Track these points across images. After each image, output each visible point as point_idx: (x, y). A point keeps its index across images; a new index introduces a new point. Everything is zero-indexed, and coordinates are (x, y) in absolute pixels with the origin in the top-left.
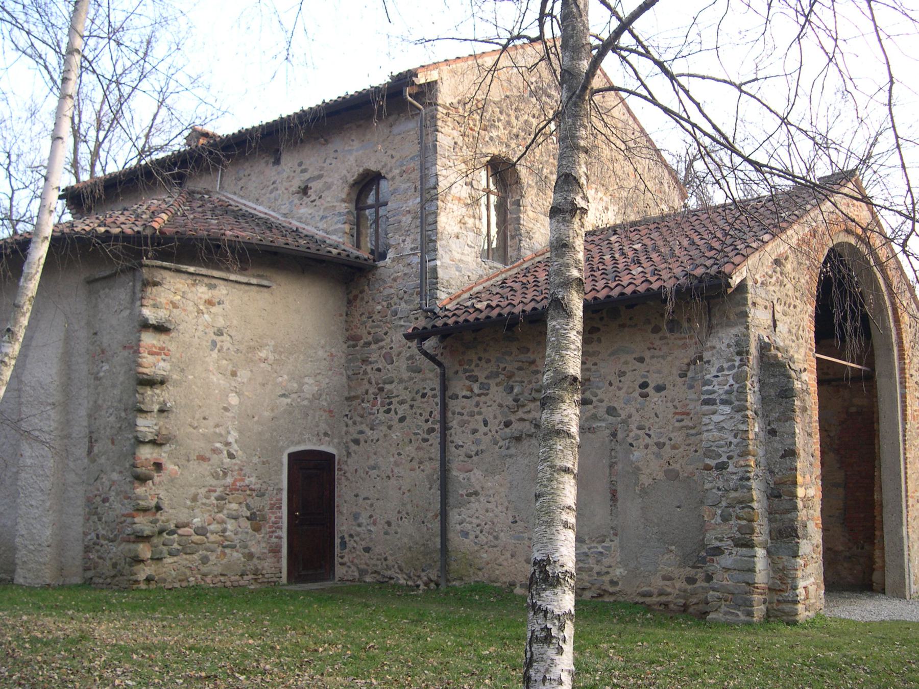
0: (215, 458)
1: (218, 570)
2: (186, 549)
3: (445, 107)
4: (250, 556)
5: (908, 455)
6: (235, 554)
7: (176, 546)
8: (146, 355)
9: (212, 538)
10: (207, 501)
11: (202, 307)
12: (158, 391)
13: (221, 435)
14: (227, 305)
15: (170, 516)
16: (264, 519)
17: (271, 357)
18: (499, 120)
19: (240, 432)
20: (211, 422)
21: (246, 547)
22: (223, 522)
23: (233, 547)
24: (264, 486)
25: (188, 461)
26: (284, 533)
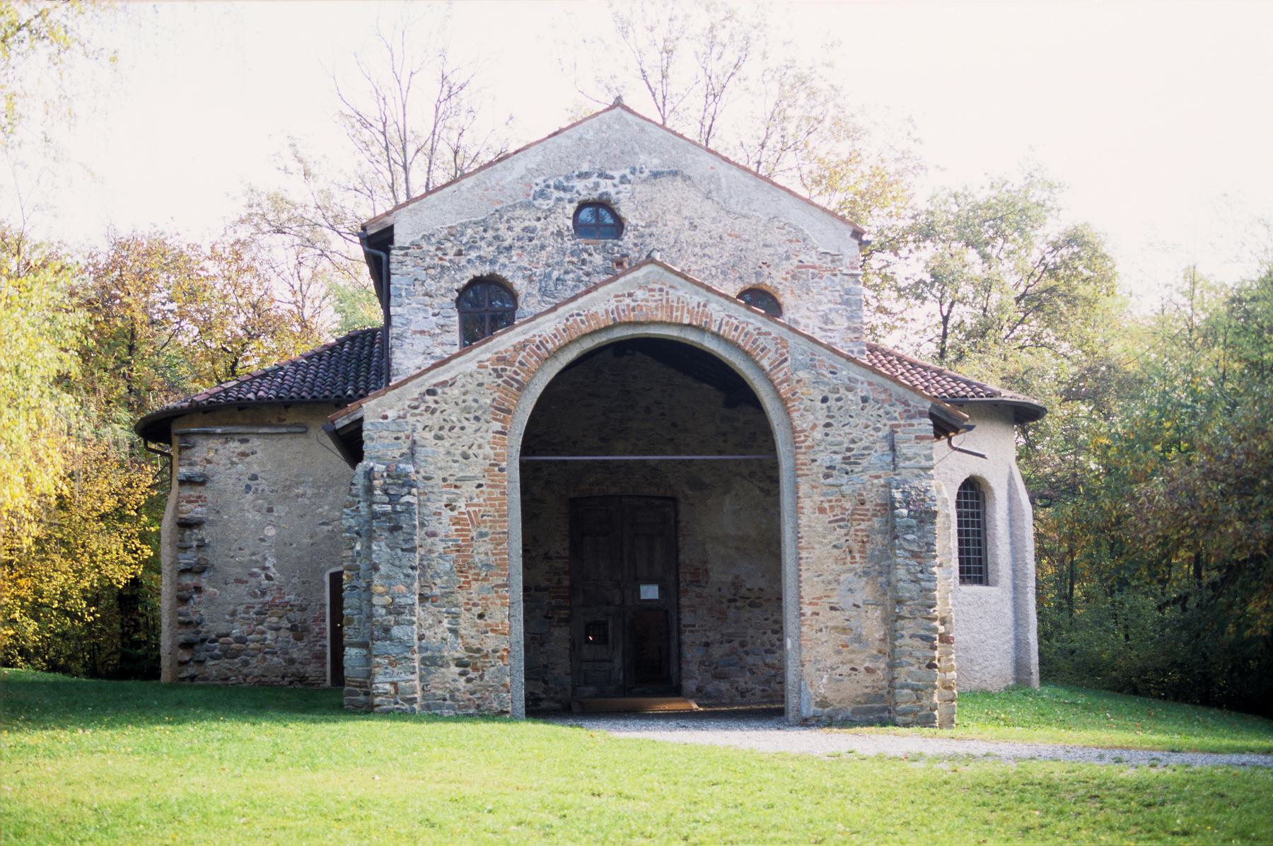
0: (253, 581)
1: (257, 672)
2: (228, 654)
3: (401, 248)
4: (292, 661)
5: (804, 554)
6: (275, 659)
7: (217, 651)
8: (184, 503)
9: (252, 645)
10: (246, 616)
11: (234, 459)
12: (196, 531)
13: (257, 562)
14: (259, 455)
15: (213, 627)
16: (306, 630)
17: (309, 492)
18: (482, 238)
19: (277, 557)
20: (247, 552)
21: (287, 653)
22: (263, 633)
23: (274, 653)
24: (305, 602)
25: (226, 584)
26: (328, 642)
